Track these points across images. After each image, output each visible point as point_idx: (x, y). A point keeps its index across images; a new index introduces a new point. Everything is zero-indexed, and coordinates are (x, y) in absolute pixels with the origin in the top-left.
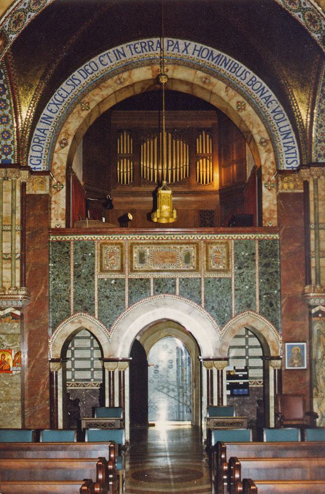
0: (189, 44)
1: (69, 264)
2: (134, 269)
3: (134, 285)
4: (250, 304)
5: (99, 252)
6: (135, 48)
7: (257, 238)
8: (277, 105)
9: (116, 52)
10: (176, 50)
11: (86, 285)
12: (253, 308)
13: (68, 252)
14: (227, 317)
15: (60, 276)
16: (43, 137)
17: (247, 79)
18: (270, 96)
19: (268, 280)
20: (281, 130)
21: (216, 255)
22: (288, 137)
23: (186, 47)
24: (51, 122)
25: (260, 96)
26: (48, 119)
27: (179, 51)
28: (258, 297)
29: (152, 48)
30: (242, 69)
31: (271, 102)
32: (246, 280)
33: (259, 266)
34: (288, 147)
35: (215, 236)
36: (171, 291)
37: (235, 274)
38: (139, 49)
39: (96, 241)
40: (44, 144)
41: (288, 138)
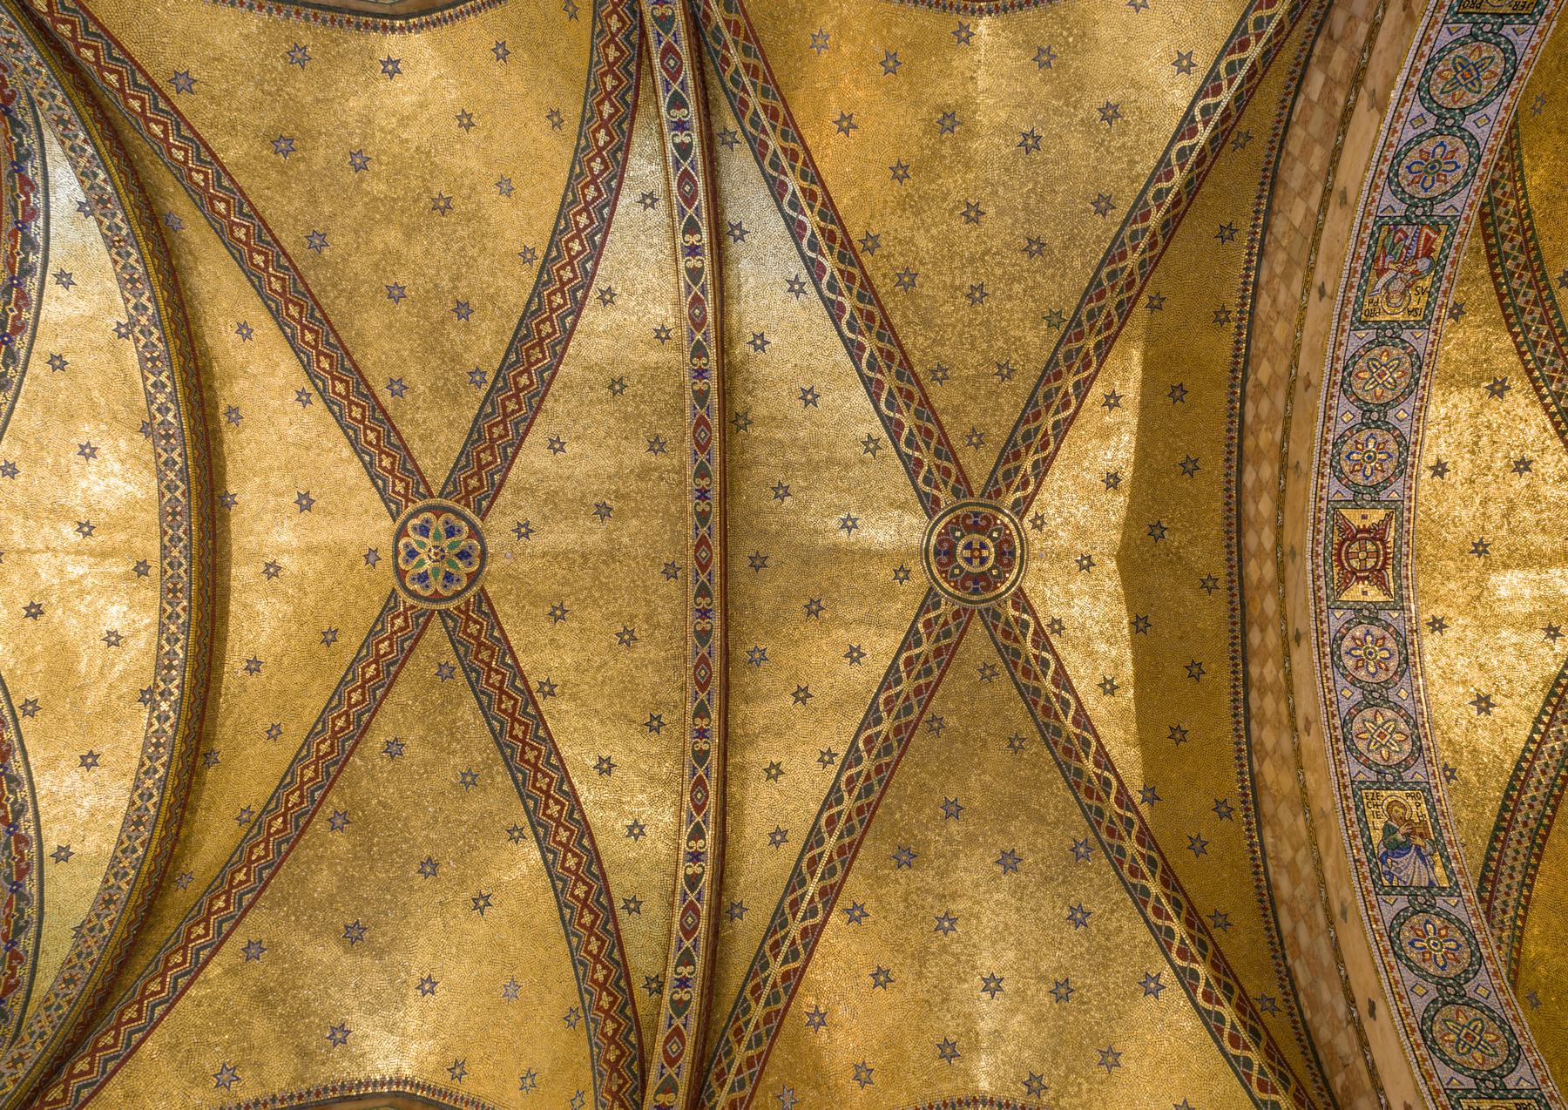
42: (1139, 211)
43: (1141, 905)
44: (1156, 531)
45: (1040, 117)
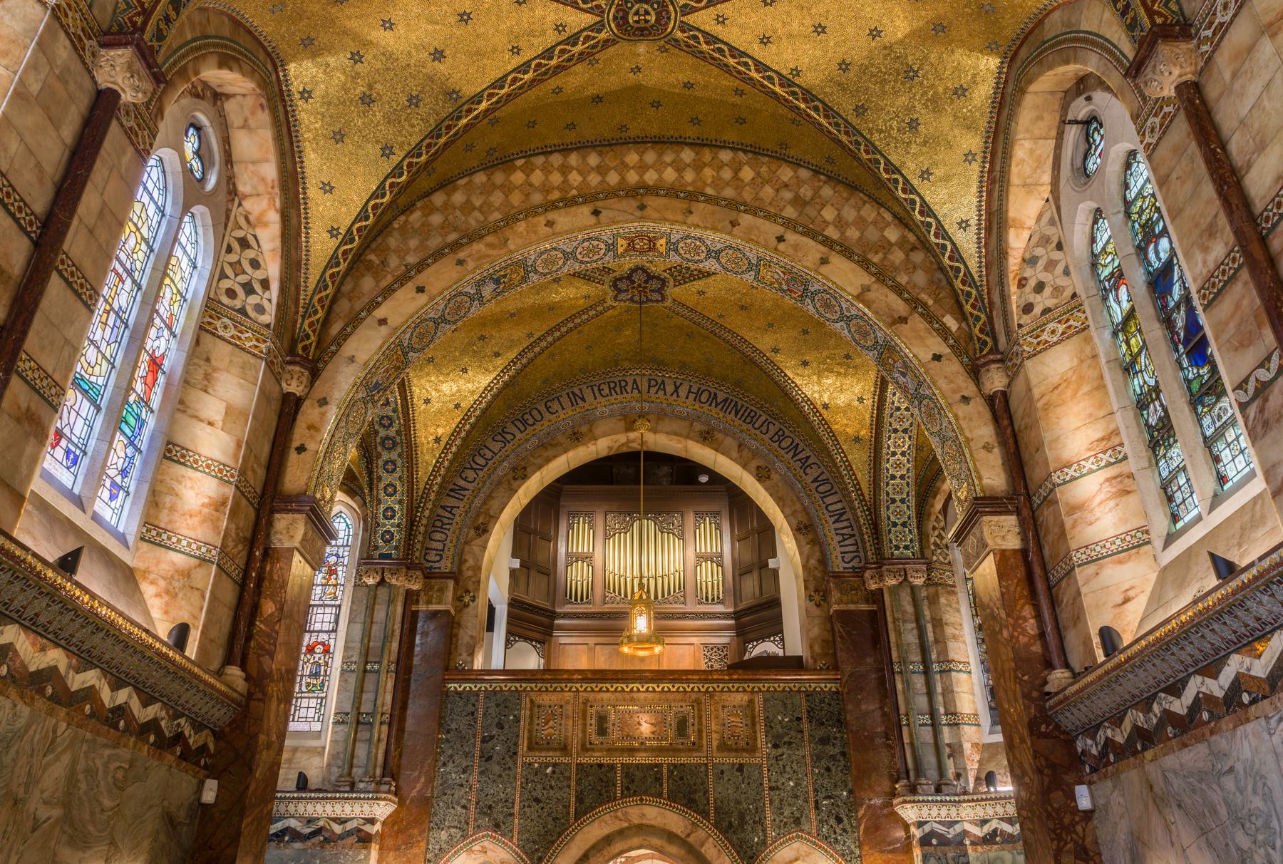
1: (474, 736)
2: (588, 746)
3: (588, 776)
4: (798, 818)
5: (528, 713)
6: (599, 390)
7: (803, 689)
8: (820, 472)
9: (571, 396)
10: (660, 393)
11: (500, 776)
12: (805, 827)
13: (473, 714)
14: (757, 843)
15: (455, 757)
17: (771, 433)
18: (808, 458)
19: (828, 769)
20: (829, 508)
23: (677, 388)
28: (812, 804)
30: (763, 418)
31: (809, 466)
32: (788, 769)
33: (810, 742)
34: (843, 535)
36: (653, 790)
37: (768, 758)
38: (606, 391)
39: (524, 694)
42: (851, 129)
43: (430, 135)
44: (656, 104)
45: (925, 82)
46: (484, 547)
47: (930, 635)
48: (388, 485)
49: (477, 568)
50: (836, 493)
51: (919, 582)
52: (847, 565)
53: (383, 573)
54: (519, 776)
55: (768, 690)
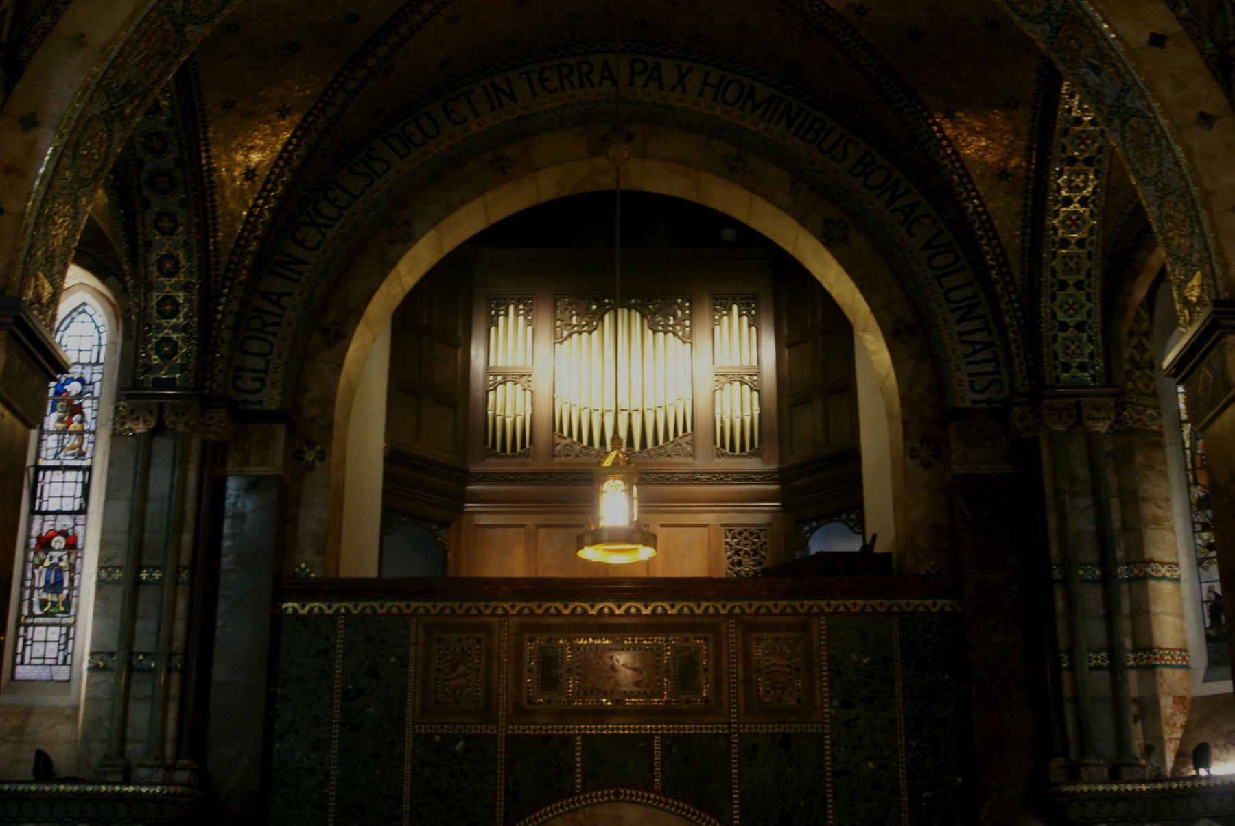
0: (690, 69)
2: (525, 705)
6: (543, 80)
7: (895, 609)
16: (275, 315)
18: (915, 206)
21: (775, 664)
22: (973, 315)
23: (682, 76)
24: (301, 274)
25: (888, 205)
26: (292, 267)
27: (661, 88)
29: (590, 80)
34: (972, 343)
35: (771, 604)
40: (275, 334)
41: (971, 319)
46: (339, 365)
47: (1116, 520)
48: (164, 257)
49: (328, 403)
50: (963, 268)
51: (1101, 427)
52: (978, 397)
53: (161, 412)
54: (408, 754)
55: (836, 613)
